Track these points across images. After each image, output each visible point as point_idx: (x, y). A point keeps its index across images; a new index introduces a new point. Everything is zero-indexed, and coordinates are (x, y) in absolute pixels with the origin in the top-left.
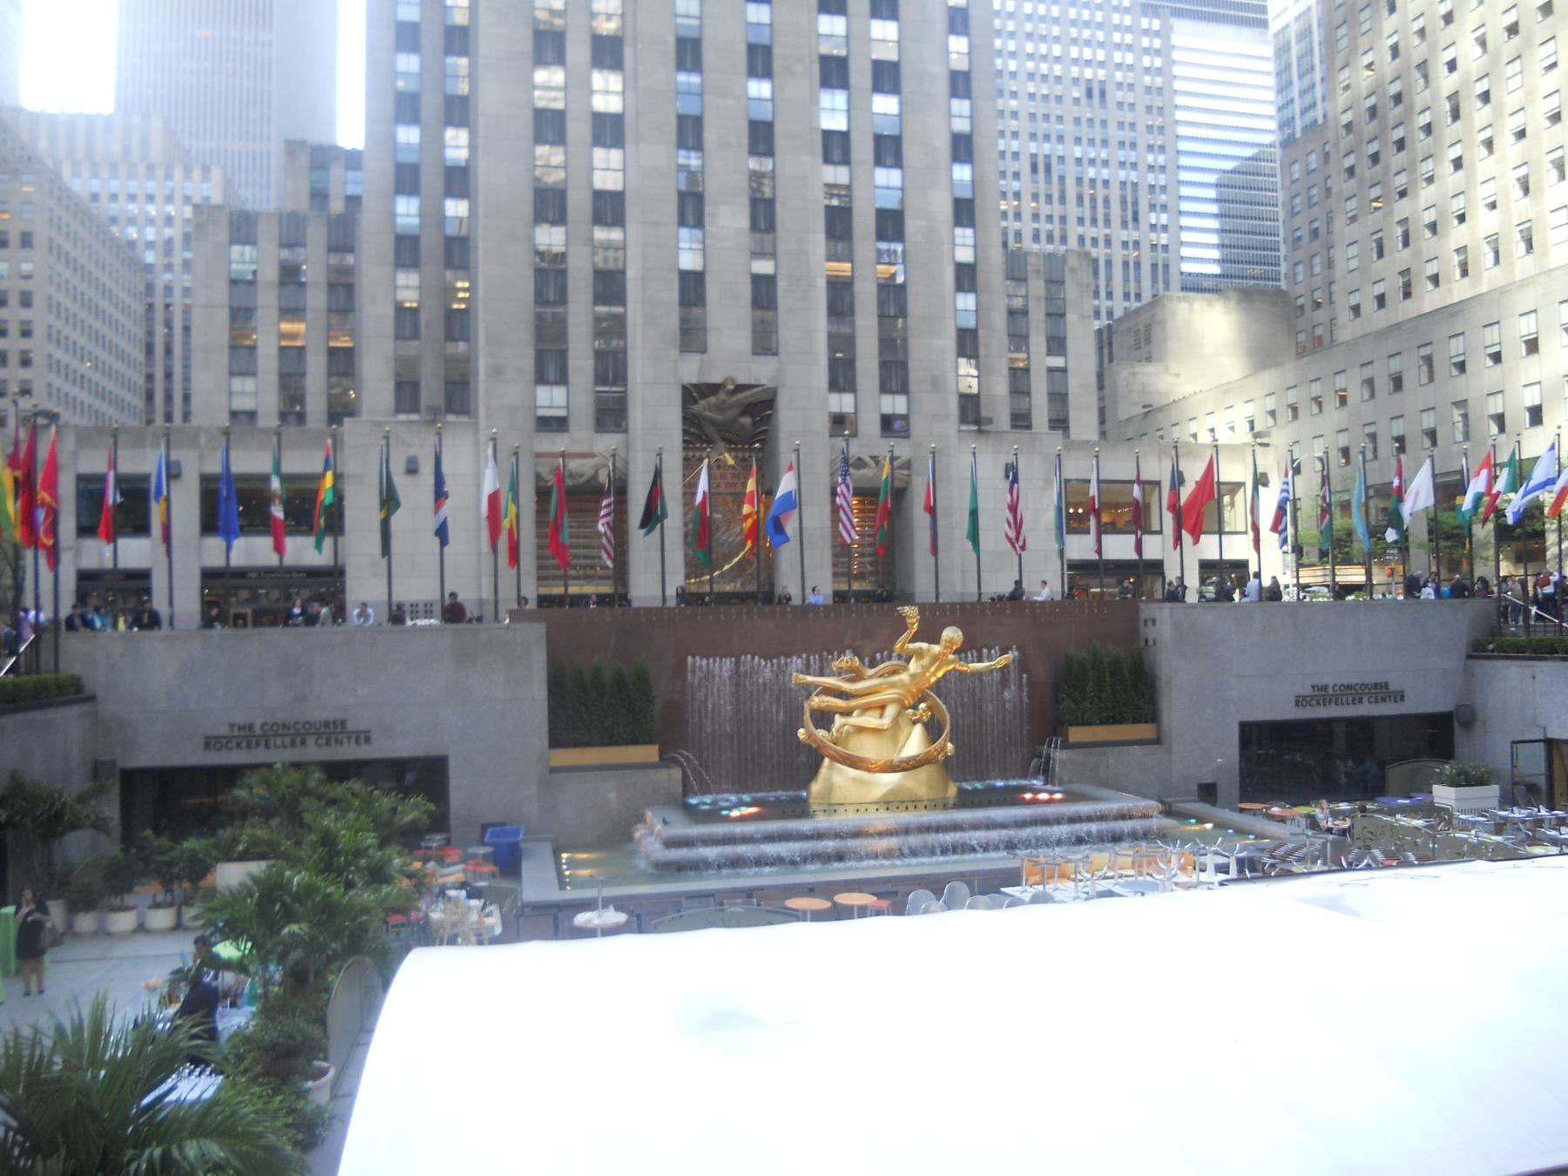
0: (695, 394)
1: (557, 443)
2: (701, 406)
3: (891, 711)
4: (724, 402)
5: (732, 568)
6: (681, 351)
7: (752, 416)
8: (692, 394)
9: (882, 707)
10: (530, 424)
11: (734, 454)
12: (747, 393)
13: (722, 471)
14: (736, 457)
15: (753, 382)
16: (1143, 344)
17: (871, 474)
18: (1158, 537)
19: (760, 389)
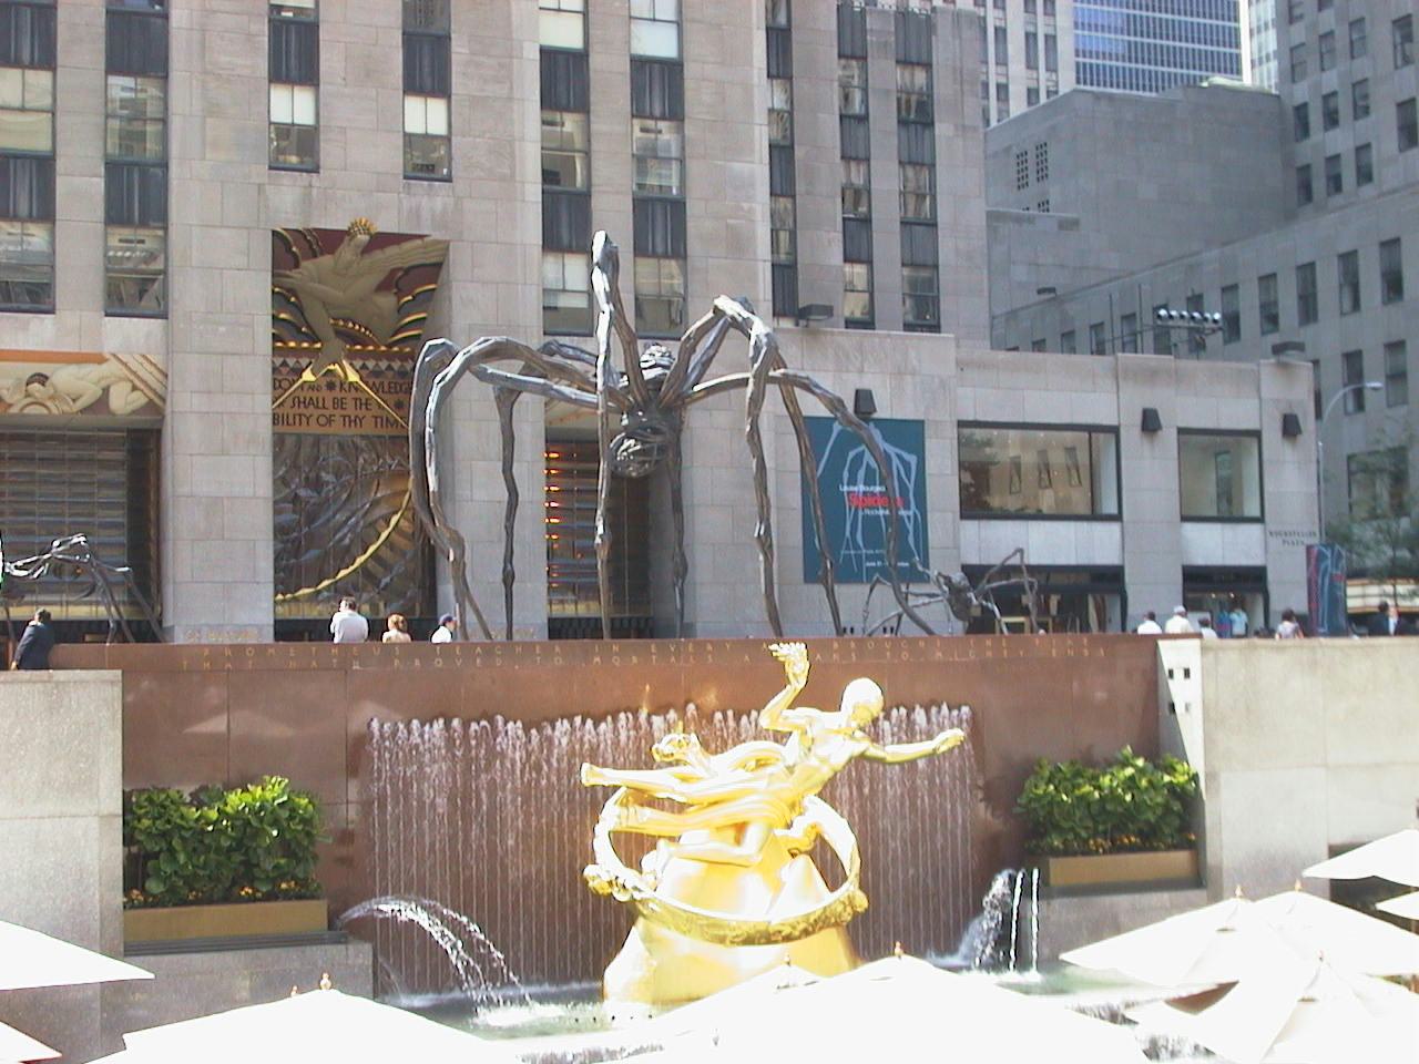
0: (294, 249)
7: (400, 294)
8: (291, 249)
11: (358, 364)
12: (392, 250)
13: (337, 393)
14: (364, 367)
18: (1115, 527)
19: (419, 242)
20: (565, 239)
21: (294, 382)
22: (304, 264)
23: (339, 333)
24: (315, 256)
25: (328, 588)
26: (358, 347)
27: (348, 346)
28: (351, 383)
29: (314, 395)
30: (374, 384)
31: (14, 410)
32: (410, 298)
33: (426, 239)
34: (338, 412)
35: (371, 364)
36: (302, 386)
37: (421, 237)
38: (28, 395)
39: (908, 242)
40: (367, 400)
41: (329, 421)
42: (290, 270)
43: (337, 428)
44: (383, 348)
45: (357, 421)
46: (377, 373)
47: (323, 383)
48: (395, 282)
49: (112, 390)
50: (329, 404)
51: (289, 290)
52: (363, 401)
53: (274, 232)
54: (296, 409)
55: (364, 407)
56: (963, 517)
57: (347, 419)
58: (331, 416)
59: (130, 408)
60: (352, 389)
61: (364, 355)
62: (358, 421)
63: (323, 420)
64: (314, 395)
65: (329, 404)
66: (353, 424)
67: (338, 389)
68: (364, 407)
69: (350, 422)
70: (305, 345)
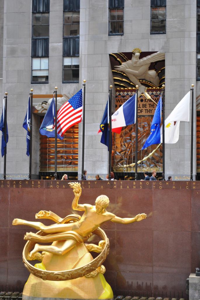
0: (118, 59)
1: (43, 90)
2: (124, 66)
3: (68, 244)
4: (136, 63)
5: (148, 159)
6: (109, 35)
10: (29, 80)
11: (150, 93)
12: (149, 57)
13: (144, 103)
14: (152, 94)
15: (150, 51)
19: (156, 54)
23: (142, 84)
24: (125, 61)
25: (140, 163)
26: (150, 88)
27: (147, 88)
28: (148, 100)
30: (155, 99)
31: (40, 112)
32: (160, 71)
33: (158, 53)
34: (144, 108)
35: (154, 93)
37: (156, 52)
38: (43, 107)
40: (153, 104)
41: (141, 111)
42: (119, 66)
44: (159, 88)
46: (156, 96)
48: (153, 66)
51: (122, 72)
52: (152, 105)
53: (110, 55)
55: (152, 107)
57: (147, 110)
58: (142, 110)
60: (149, 101)
61: (152, 90)
62: (150, 111)
66: (149, 112)
67: (144, 101)
68: (152, 107)
69: (148, 111)
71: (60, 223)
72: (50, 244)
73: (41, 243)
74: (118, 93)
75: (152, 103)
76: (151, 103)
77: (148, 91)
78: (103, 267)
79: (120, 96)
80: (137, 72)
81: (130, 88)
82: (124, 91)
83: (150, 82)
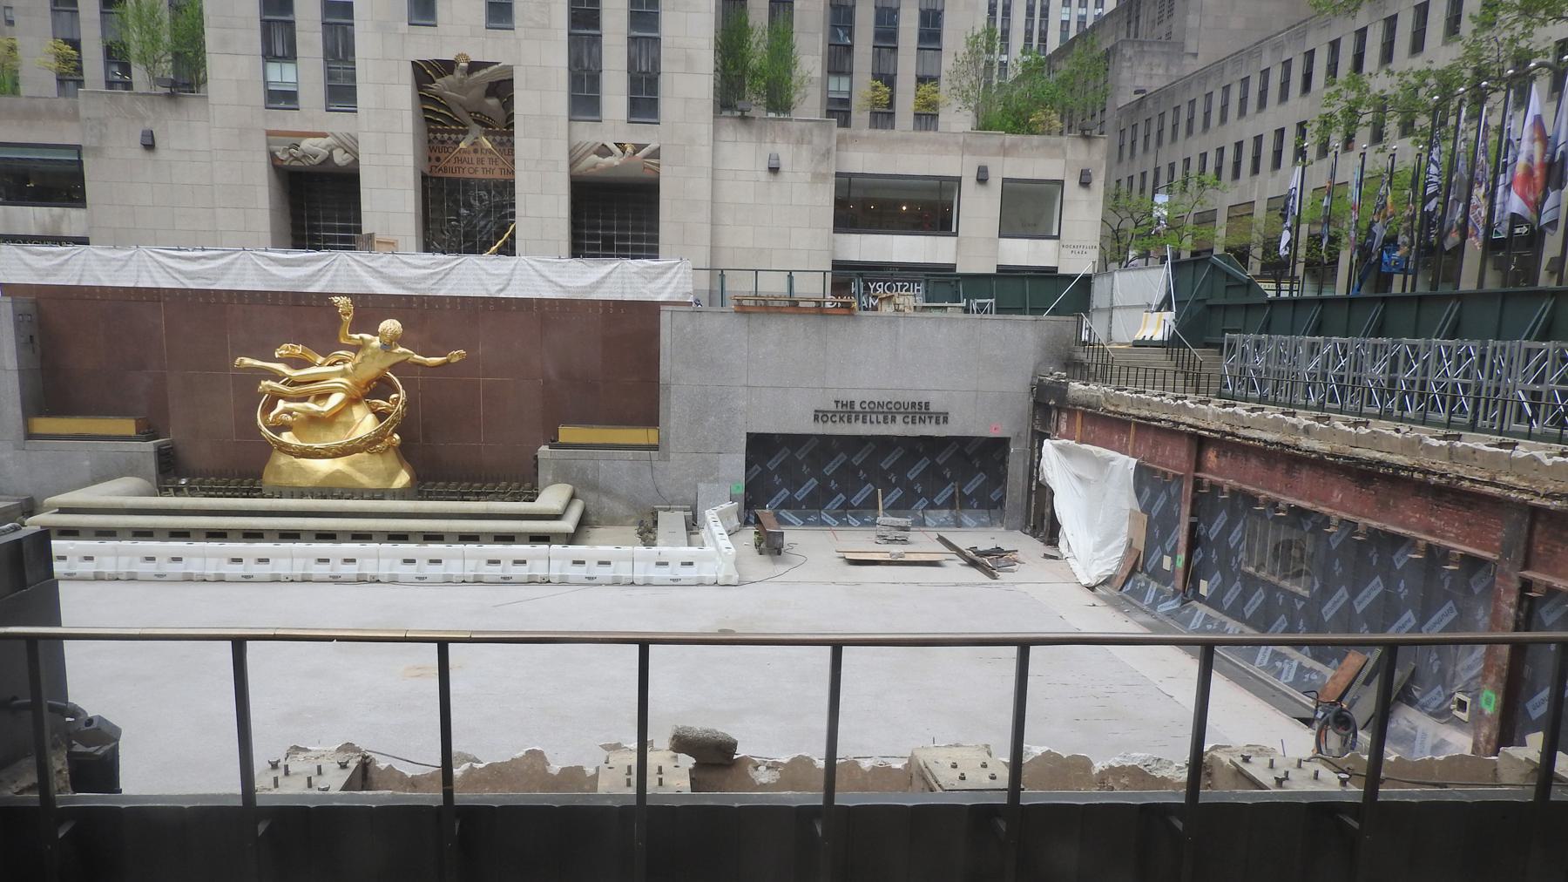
3: (336, 399)
9: (329, 395)
11: (491, 137)
13: (479, 155)
16: (1165, 17)
17: (617, 163)
20: (586, 65)
21: (455, 149)
22: (438, 80)
28: (487, 150)
29: (466, 156)
34: (481, 166)
35: (498, 138)
36: (459, 151)
38: (291, 155)
39: (920, 61)
41: (475, 171)
43: (480, 175)
45: (491, 171)
47: (471, 149)
49: (334, 152)
50: (475, 161)
54: (456, 165)
56: (834, 232)
59: (344, 163)
63: (471, 171)
64: (466, 156)
65: (475, 161)
70: (460, 128)
71: (320, 365)
72: (305, 399)
73: (288, 399)
74: (432, 135)
75: (494, 157)
76: (492, 156)
77: (486, 134)
78: (396, 436)
79: (435, 141)
80: (464, 98)
81: (453, 127)
82: (442, 132)
83: (489, 118)
